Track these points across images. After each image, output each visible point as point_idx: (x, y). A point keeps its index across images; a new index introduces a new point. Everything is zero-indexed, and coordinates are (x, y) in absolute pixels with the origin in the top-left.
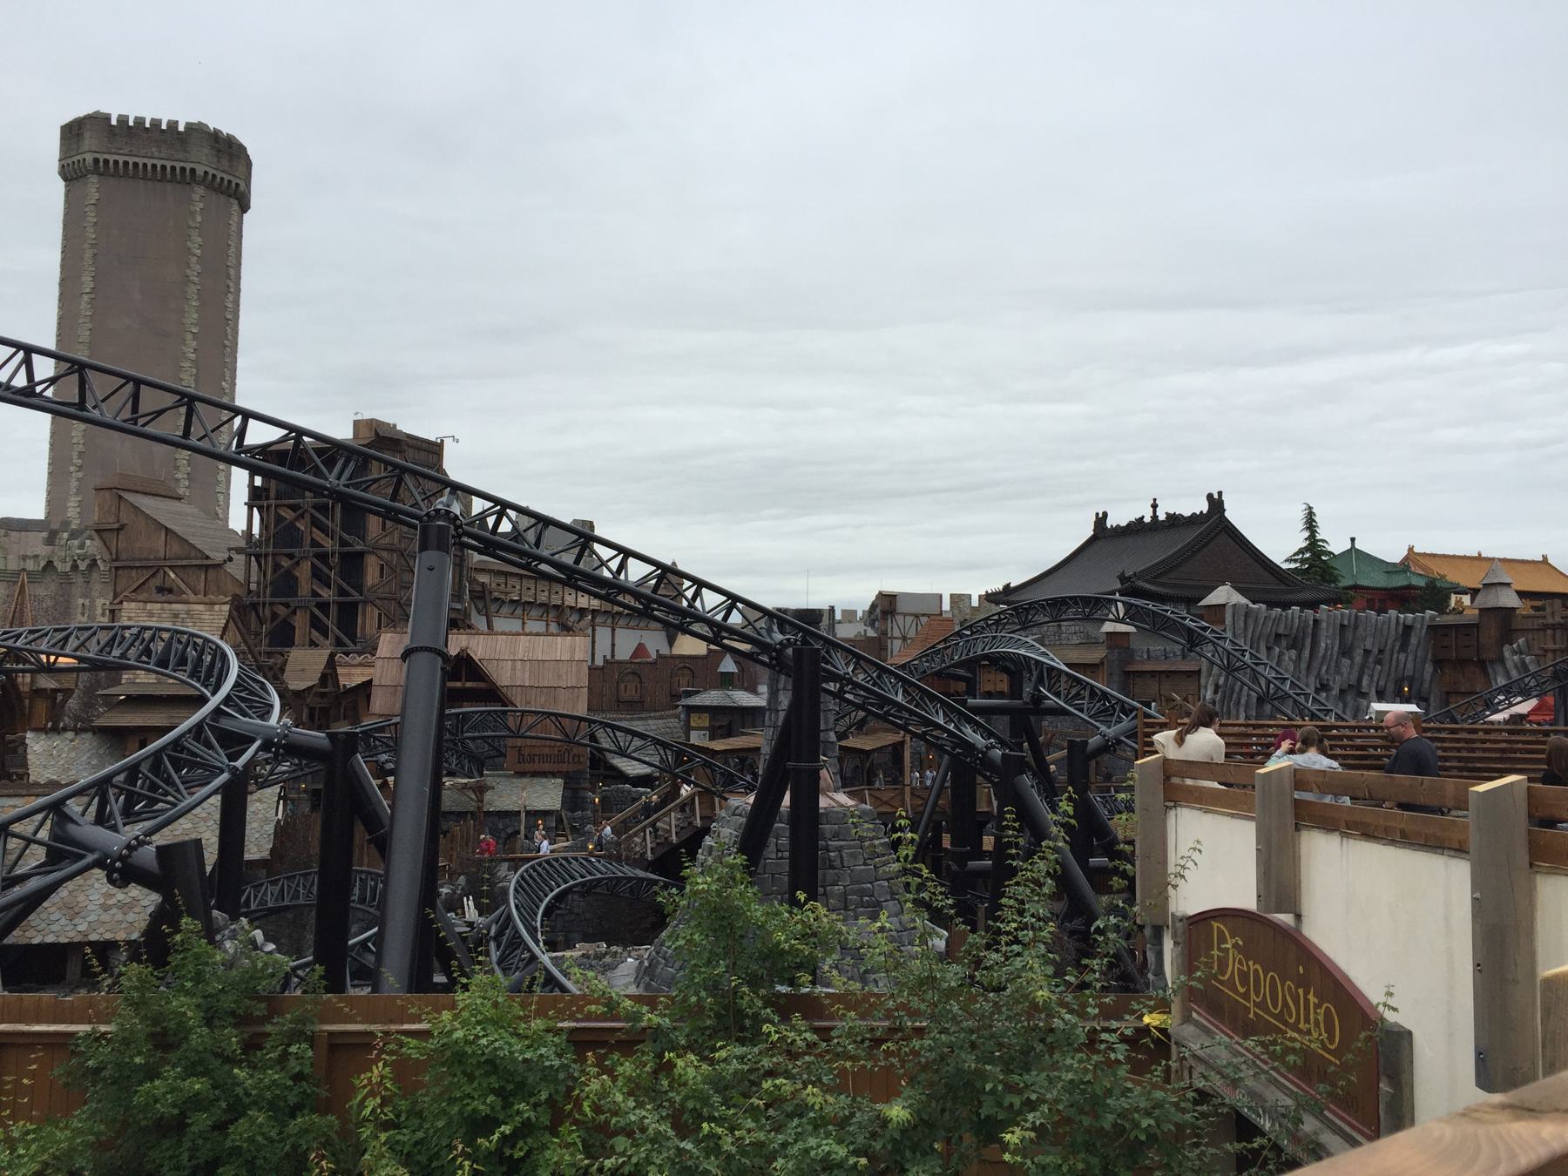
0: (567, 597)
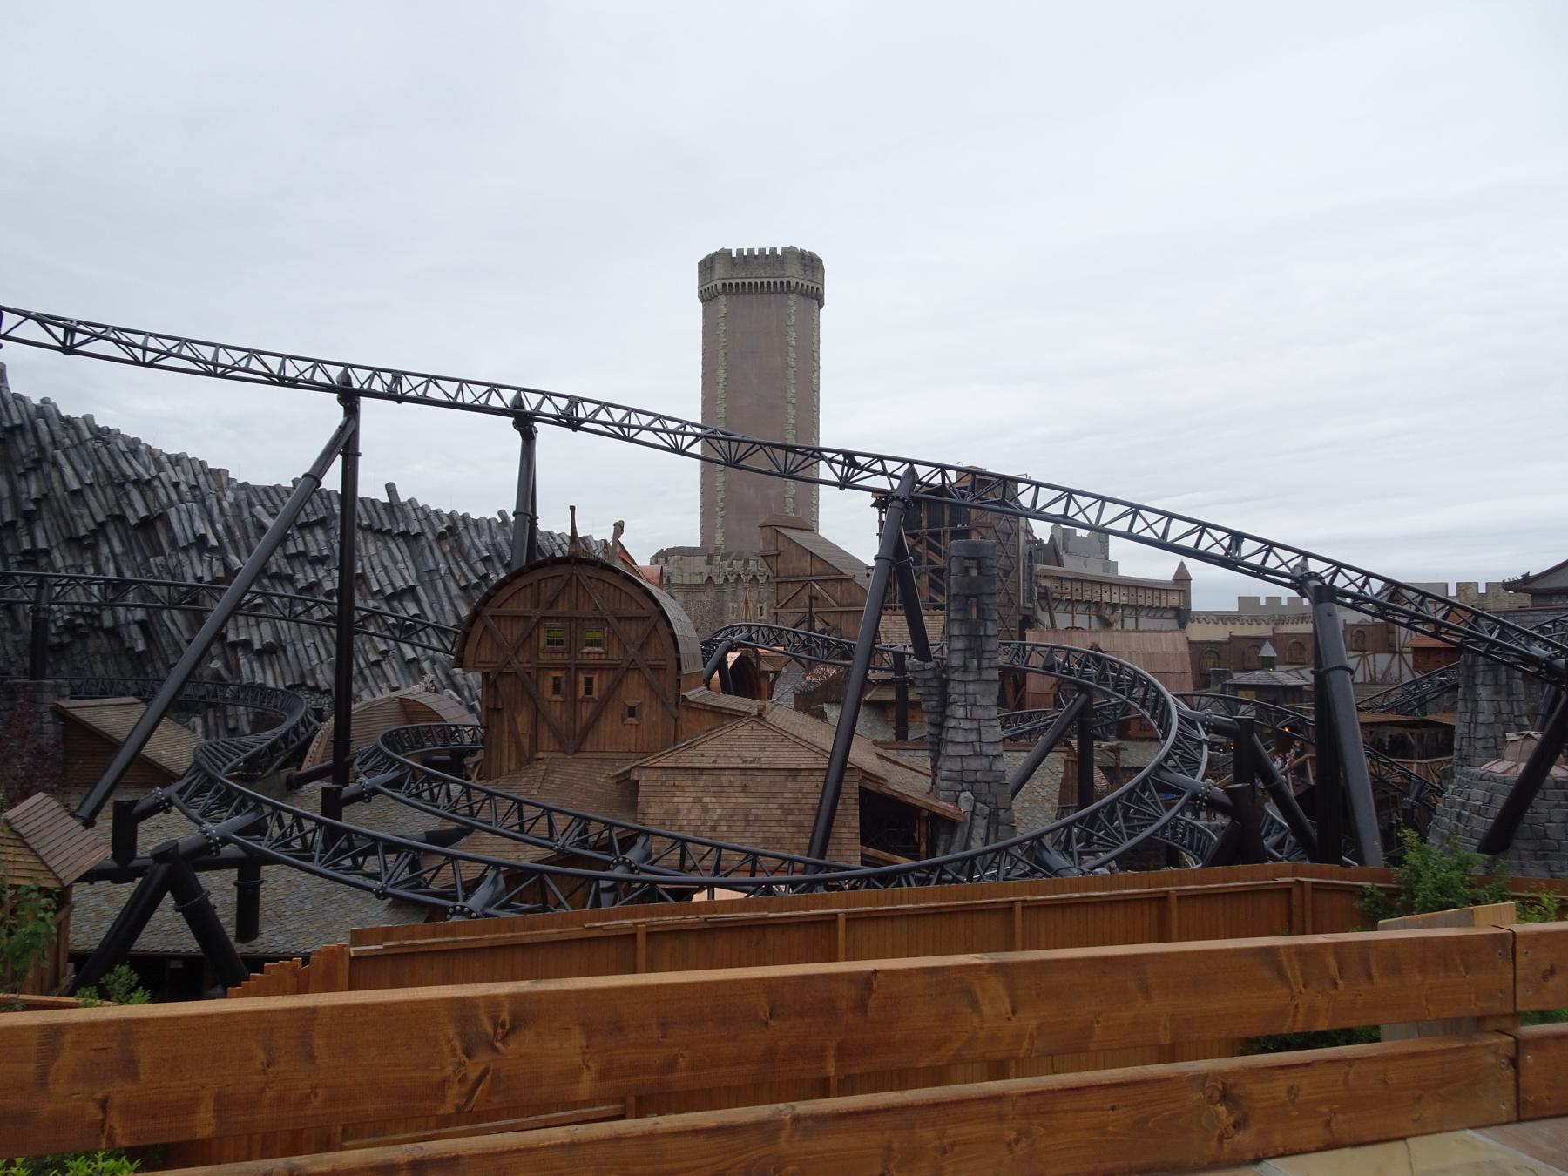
0: (1113, 596)
